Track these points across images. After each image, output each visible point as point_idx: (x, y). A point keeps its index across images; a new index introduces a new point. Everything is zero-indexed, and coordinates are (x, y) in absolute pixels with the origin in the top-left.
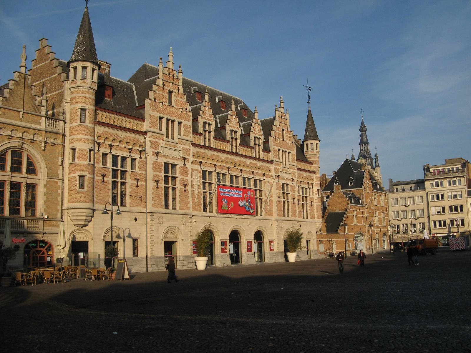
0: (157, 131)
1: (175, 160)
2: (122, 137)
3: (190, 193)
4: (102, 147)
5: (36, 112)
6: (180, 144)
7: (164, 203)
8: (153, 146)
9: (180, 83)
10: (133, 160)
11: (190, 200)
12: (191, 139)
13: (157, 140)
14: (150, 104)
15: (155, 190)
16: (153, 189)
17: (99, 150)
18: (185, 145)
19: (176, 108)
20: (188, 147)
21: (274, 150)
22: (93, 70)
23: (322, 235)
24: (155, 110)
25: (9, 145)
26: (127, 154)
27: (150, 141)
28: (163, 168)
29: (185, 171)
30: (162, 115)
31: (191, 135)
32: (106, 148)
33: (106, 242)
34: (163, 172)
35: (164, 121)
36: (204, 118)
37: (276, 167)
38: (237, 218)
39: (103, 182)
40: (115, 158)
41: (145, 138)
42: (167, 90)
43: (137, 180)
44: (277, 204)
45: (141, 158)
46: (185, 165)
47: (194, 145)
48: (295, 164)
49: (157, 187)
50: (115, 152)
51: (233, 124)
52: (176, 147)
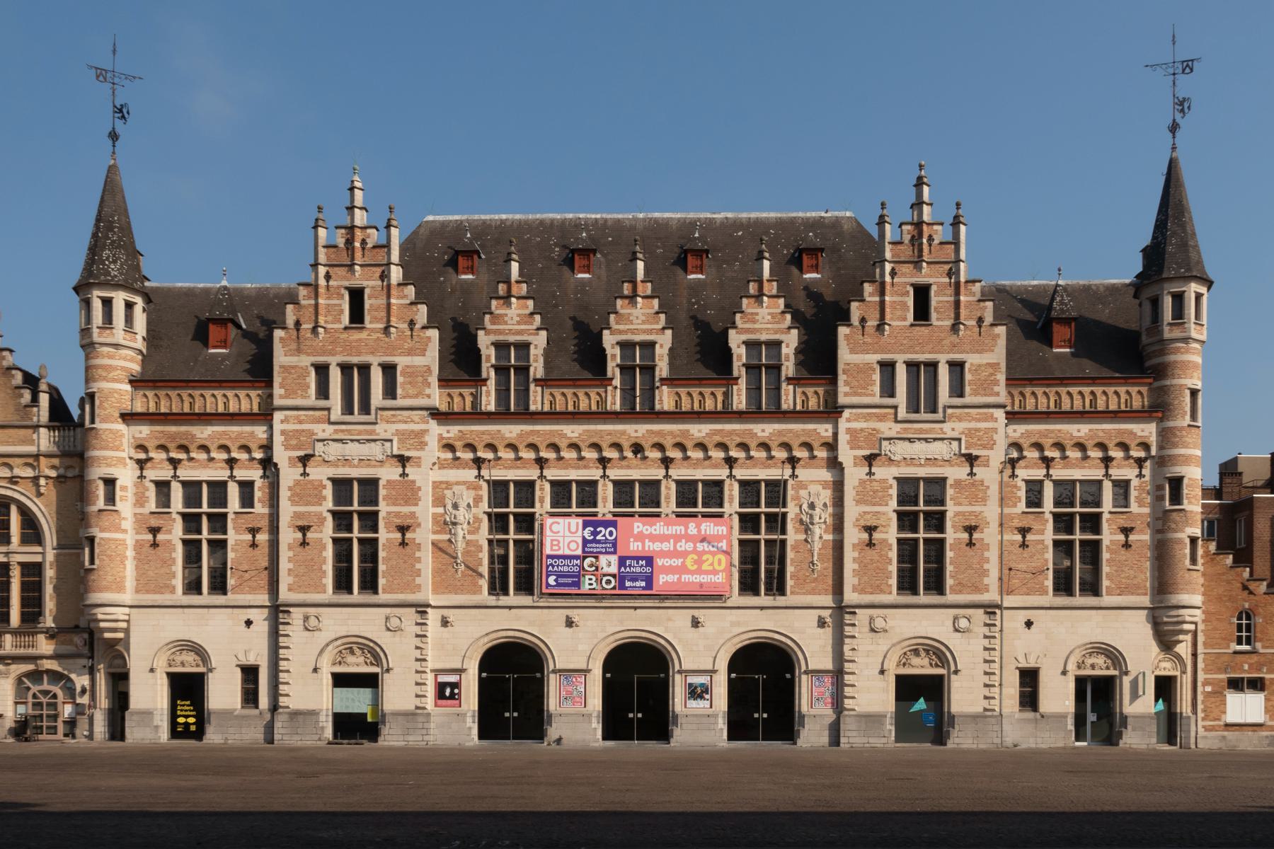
1: (368, 466)
2: (205, 435)
4: (153, 468)
6: (388, 422)
8: (294, 442)
14: (281, 338)
15: (300, 549)
16: (290, 548)
18: (406, 422)
19: (373, 330)
20: (423, 427)
21: (865, 369)
23: (1255, 658)
24: (299, 351)
26: (221, 474)
27: (283, 432)
29: (408, 493)
30: (321, 359)
32: (162, 468)
35: (335, 377)
38: (635, 608)
39: (155, 545)
41: (271, 427)
42: (339, 287)
43: (254, 531)
44: (856, 554)
46: (404, 475)
49: (304, 543)
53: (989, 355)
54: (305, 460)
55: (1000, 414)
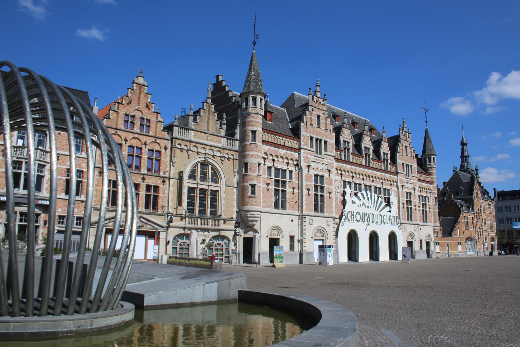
0: (309, 148)
3: (334, 199)
4: (268, 161)
5: (218, 133)
7: (314, 208)
9: (325, 109)
10: (291, 172)
11: (334, 205)
12: (334, 155)
13: (308, 156)
15: (307, 196)
17: (265, 164)
20: (332, 162)
22: (261, 100)
24: (307, 131)
25: (199, 160)
26: (285, 167)
27: (303, 157)
28: (313, 178)
30: (312, 135)
31: (334, 151)
33: (270, 238)
34: (313, 182)
35: (314, 140)
36: (344, 137)
37: (401, 178)
39: (268, 190)
40: (277, 169)
43: (293, 188)
45: (296, 170)
47: (337, 160)
48: (416, 176)
49: (309, 195)
50: (277, 165)
51: (367, 142)
52: (323, 161)
53: (415, 165)
54: (309, 166)
55: (417, 179)
